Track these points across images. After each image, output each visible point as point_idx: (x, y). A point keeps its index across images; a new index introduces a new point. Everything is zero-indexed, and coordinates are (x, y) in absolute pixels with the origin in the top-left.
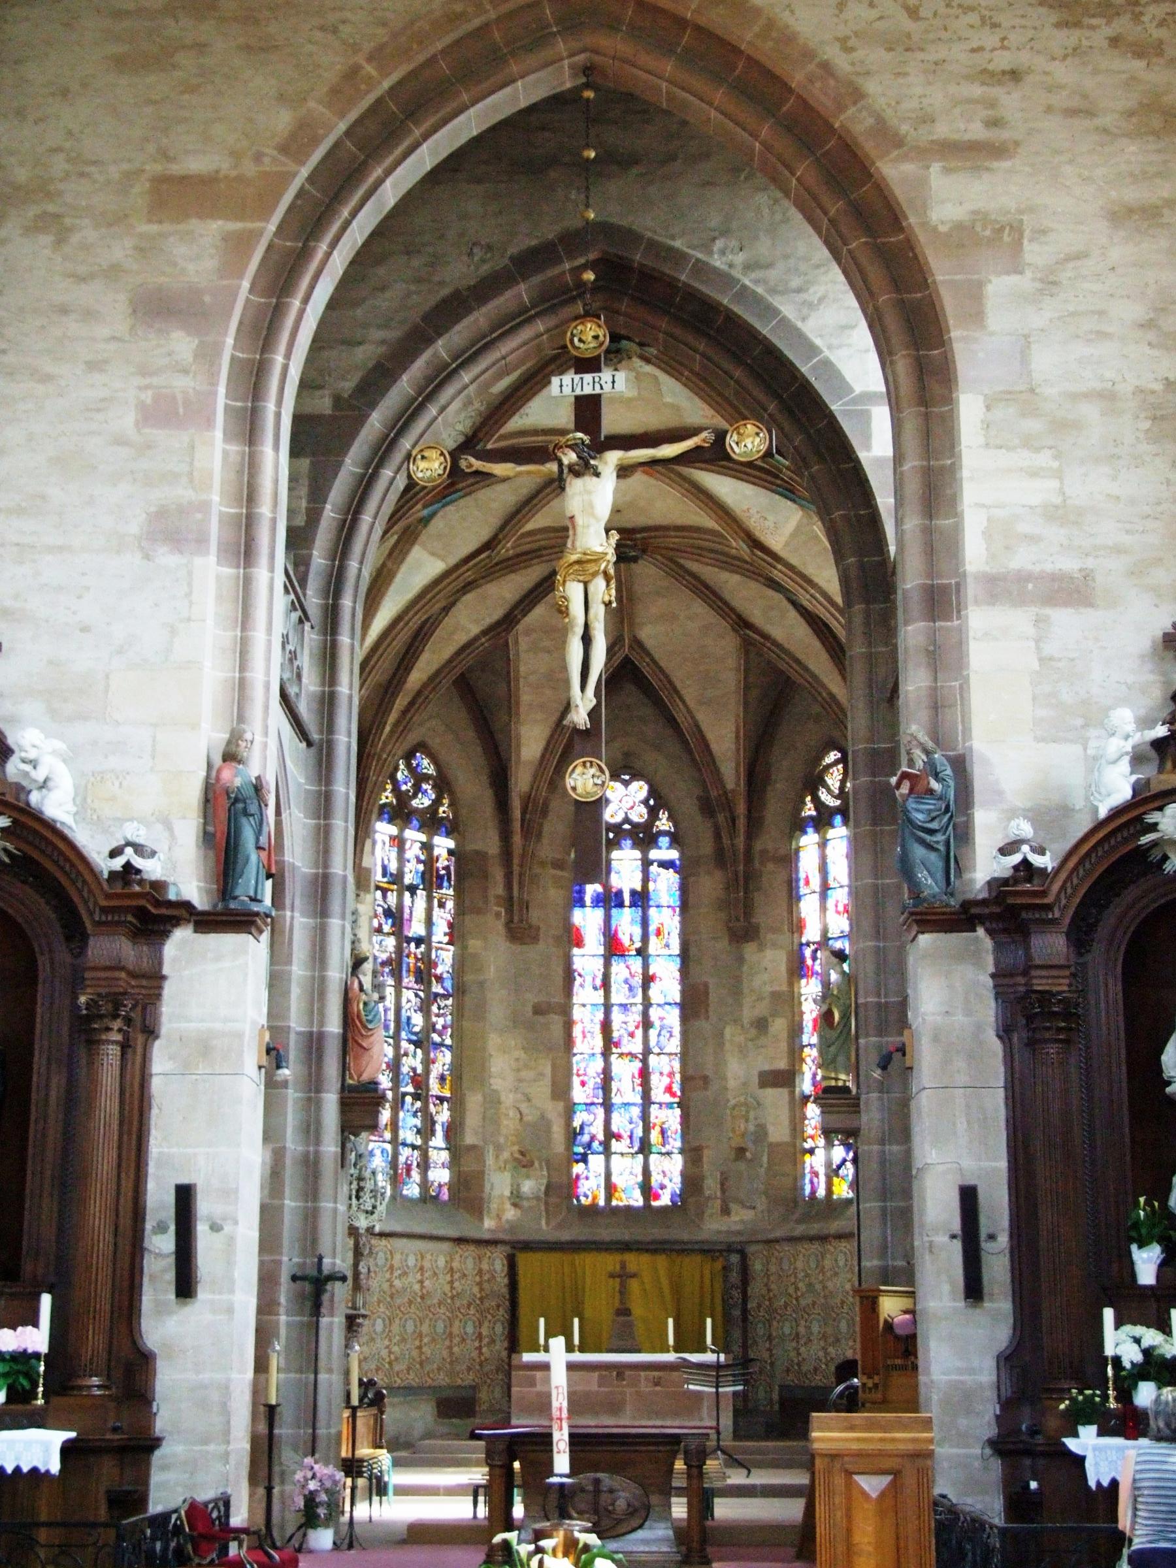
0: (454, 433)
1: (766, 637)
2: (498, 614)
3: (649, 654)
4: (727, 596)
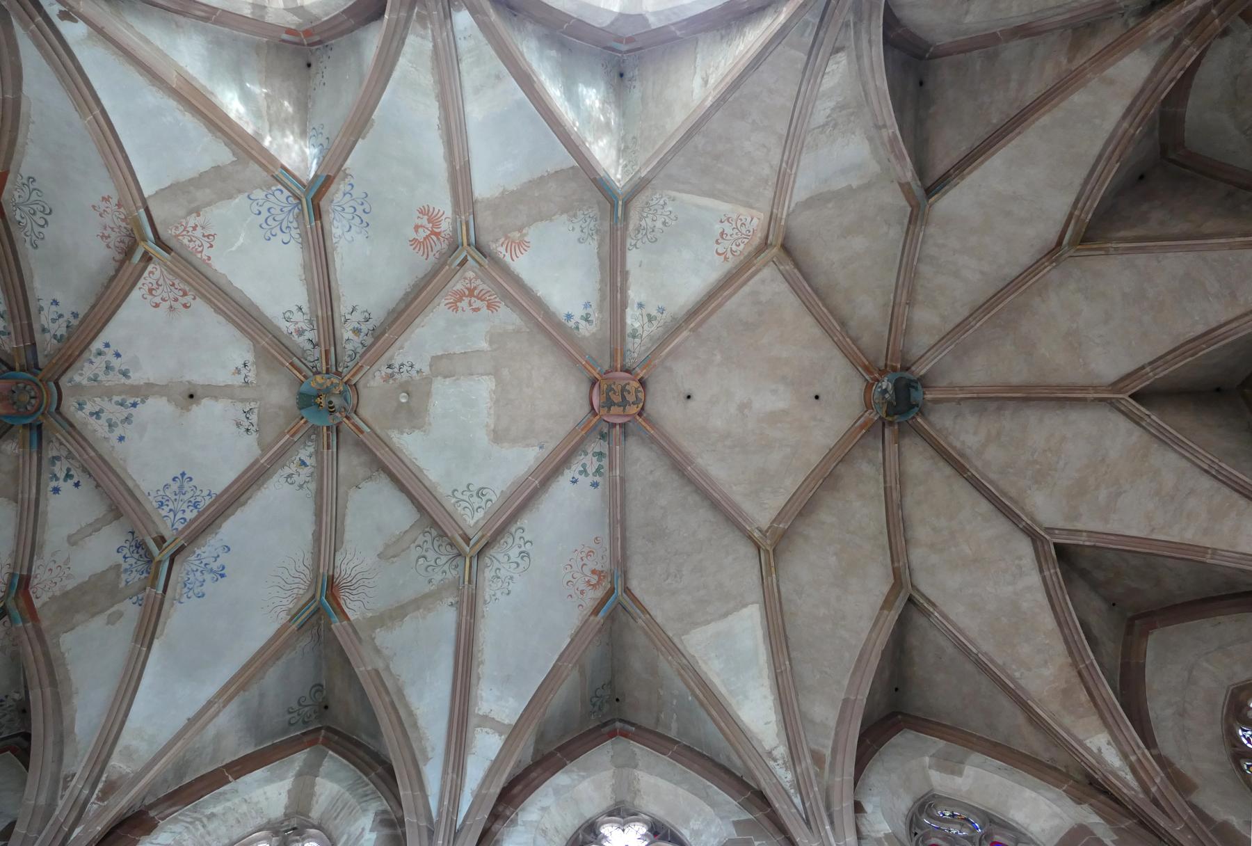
0: (446, 568)
1: (1071, 216)
2: (1024, 547)
3: (1143, 368)
4: (1014, 271)
